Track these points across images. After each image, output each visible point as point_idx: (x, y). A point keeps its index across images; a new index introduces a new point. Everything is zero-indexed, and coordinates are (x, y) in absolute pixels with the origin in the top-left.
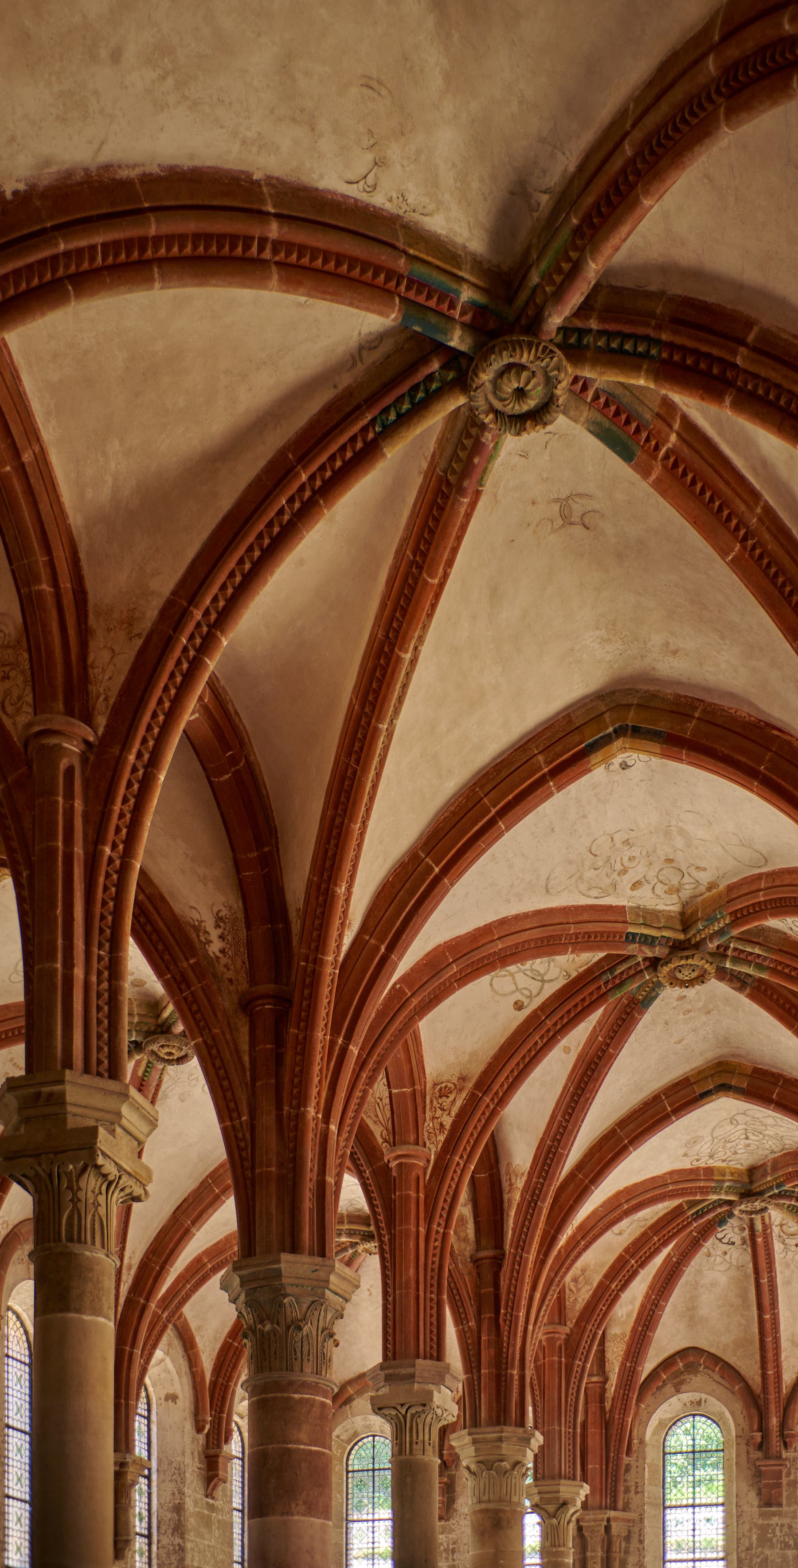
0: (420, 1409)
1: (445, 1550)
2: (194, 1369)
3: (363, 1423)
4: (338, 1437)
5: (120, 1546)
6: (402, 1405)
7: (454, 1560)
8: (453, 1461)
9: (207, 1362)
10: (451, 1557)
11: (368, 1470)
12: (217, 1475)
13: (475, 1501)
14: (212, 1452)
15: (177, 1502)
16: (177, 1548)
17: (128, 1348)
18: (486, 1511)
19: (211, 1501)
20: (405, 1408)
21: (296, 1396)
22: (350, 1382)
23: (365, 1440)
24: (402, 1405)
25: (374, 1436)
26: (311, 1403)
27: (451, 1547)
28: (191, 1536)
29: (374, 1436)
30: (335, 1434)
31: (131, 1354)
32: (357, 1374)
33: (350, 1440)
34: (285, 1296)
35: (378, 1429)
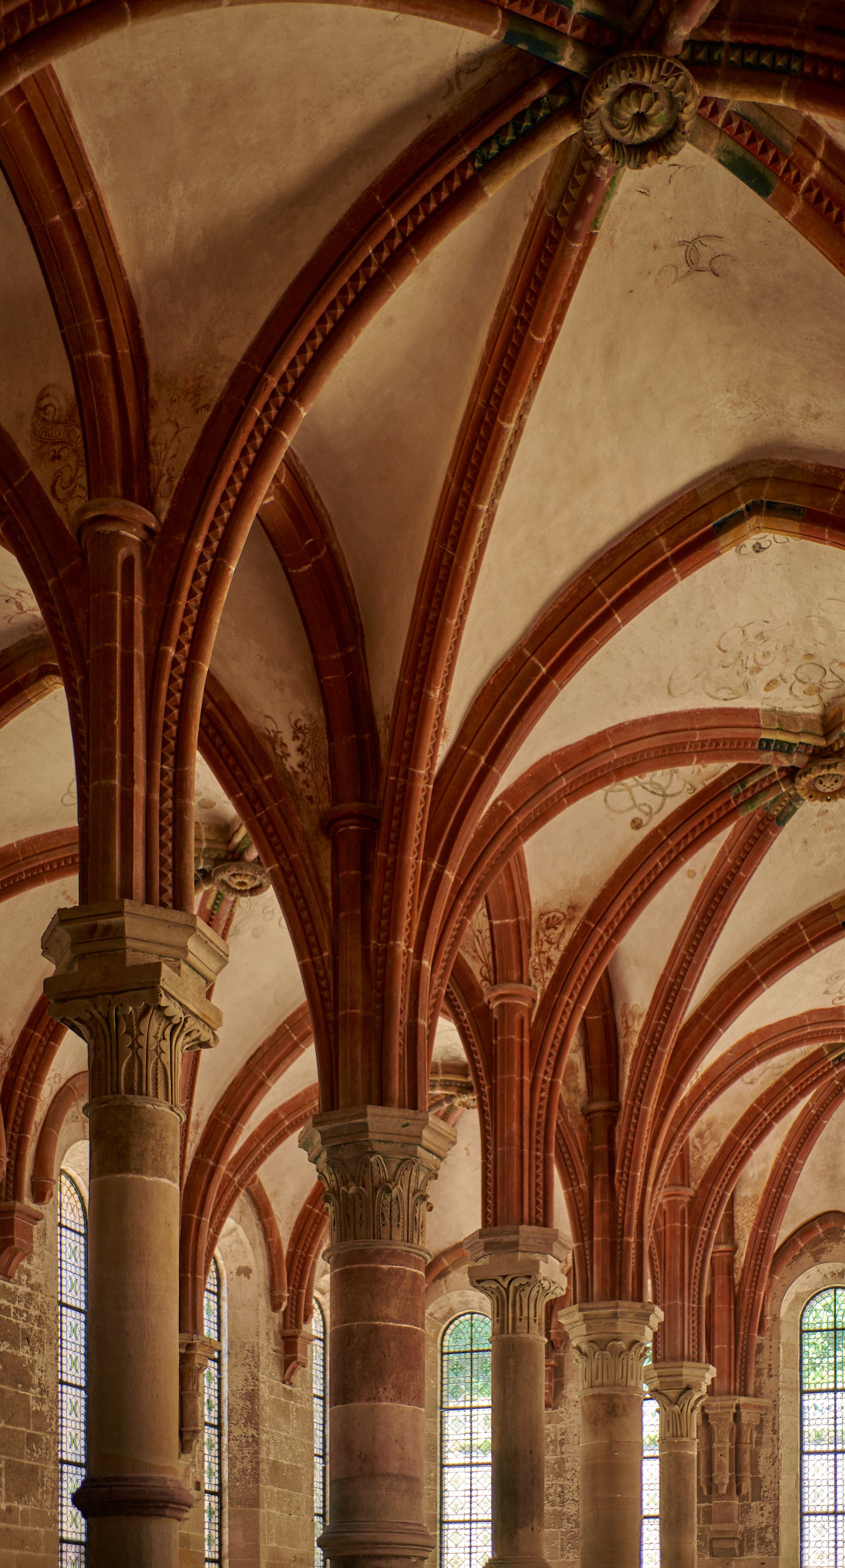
0: (524, 1281)
1: (552, 1441)
2: (270, 1240)
3: (460, 1299)
4: (431, 1315)
5: (187, 1437)
6: (504, 1277)
8: (561, 1341)
9: (284, 1232)
11: (465, 1352)
12: (295, 1358)
13: (586, 1385)
14: (290, 1332)
15: (250, 1388)
16: (250, 1440)
17: (195, 1216)
18: (599, 1396)
19: (288, 1387)
20: (508, 1279)
21: (384, 1266)
22: (445, 1253)
23: (462, 1318)
24: (504, 1277)
25: (472, 1313)
26: (401, 1275)
27: (559, 1438)
28: (266, 1426)
29: (472, 1313)
30: (428, 1311)
31: (199, 1222)
32: (453, 1244)
33: (445, 1319)
34: (373, 1153)
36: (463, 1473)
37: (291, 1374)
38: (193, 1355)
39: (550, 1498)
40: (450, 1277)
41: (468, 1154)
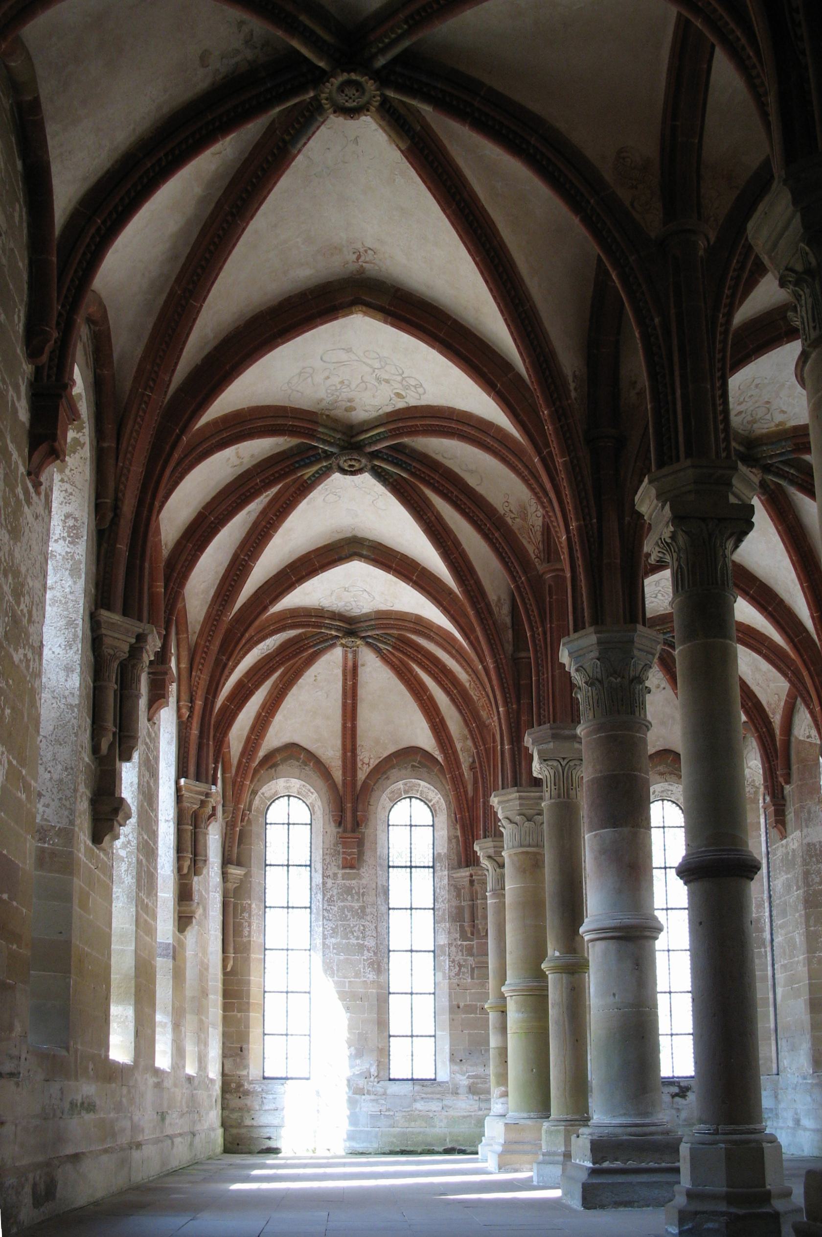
0: (577, 762)
3: (285, 784)
4: (263, 794)
6: (564, 759)
10: (361, 899)
18: (527, 853)
20: (566, 761)
21: (638, 734)
27: (361, 891)
33: (271, 797)
35: (296, 790)
39: (355, 934)
40: (281, 767)
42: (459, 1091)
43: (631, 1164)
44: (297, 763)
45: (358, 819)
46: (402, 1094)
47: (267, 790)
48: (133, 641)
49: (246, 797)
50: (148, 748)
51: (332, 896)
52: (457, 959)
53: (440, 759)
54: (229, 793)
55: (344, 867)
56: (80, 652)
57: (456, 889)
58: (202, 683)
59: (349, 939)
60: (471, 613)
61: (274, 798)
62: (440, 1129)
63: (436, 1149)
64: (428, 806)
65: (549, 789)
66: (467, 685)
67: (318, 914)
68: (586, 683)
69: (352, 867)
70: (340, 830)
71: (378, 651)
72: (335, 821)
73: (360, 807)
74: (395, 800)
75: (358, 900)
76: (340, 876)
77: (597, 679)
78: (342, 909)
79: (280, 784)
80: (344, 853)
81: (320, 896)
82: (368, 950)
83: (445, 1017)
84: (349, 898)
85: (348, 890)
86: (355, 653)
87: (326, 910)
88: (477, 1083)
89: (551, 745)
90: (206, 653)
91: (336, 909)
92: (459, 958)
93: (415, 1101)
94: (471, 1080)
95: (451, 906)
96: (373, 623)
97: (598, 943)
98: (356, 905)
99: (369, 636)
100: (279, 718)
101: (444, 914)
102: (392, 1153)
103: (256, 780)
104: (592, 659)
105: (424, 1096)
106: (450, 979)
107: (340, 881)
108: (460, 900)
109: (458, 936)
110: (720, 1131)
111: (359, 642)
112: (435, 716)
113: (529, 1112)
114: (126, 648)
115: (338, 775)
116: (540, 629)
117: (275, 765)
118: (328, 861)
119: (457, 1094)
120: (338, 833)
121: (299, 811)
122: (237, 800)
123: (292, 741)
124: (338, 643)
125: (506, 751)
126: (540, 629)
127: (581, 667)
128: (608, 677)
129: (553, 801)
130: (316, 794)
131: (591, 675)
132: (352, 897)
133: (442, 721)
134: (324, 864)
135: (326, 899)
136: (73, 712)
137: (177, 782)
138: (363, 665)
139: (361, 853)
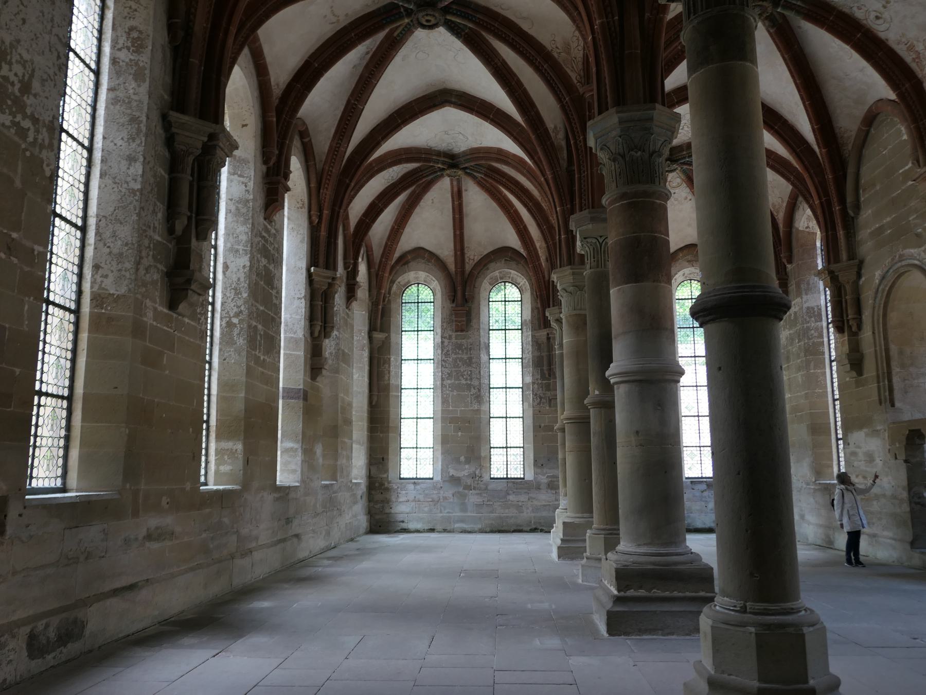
3: (415, 276)
4: (399, 282)
5: (328, 330)
6: (601, 237)
7: (471, 354)
11: (415, 303)
21: (658, 201)
25: (418, 284)
27: (469, 347)
31: (339, 212)
33: (405, 285)
36: (413, 364)
37: (350, 304)
38: (334, 284)
41: (433, 203)
42: (541, 487)
43: (657, 593)
44: (423, 261)
45: (467, 297)
46: (499, 489)
47: (402, 279)
48: (206, 139)
49: (386, 284)
50: (266, 241)
51: (448, 351)
52: (538, 393)
53: (524, 255)
54: (374, 283)
55: (456, 331)
56: (143, 144)
57: (536, 344)
58: (328, 197)
59: (461, 380)
60: (533, 137)
61: (408, 285)
62: (527, 515)
63: (525, 529)
64: (518, 288)
65: (589, 261)
66: (539, 199)
67: (438, 363)
68: (609, 159)
69: (462, 331)
70: (454, 305)
71: (474, 178)
72: (450, 299)
73: (468, 288)
74: (494, 283)
75: (467, 353)
76: (453, 336)
77: (619, 154)
78: (455, 360)
79: (411, 275)
80: (456, 321)
81: (439, 351)
82: (474, 388)
83: (531, 434)
84: (460, 352)
85: (459, 347)
86: (459, 181)
87: (444, 360)
88: (554, 482)
89: (590, 226)
90: (330, 175)
91: (451, 360)
92: (540, 392)
93: (508, 494)
94: (550, 479)
95: (533, 357)
96: (468, 157)
97: (622, 386)
98: (465, 357)
99: (466, 168)
100: (408, 229)
101: (529, 362)
102: (492, 532)
103: (394, 272)
104: (615, 137)
105: (515, 490)
106: (533, 407)
107: (454, 340)
108: (540, 352)
109: (539, 377)
110: (748, 610)
111: (460, 172)
112: (520, 223)
113: (582, 513)
114: (200, 145)
115: (452, 267)
116: (581, 137)
117: (407, 263)
118: (445, 327)
119: (540, 489)
120: (452, 307)
121: (426, 294)
122: (379, 288)
123: (419, 246)
124: (445, 174)
125: (563, 240)
126: (581, 137)
127: (606, 146)
128: (629, 152)
129: (592, 270)
130: (436, 282)
131: (614, 151)
132: (463, 351)
133: (525, 227)
134: (442, 329)
135: (444, 353)
136: (135, 195)
137: (308, 270)
138: (466, 190)
139: (469, 321)
